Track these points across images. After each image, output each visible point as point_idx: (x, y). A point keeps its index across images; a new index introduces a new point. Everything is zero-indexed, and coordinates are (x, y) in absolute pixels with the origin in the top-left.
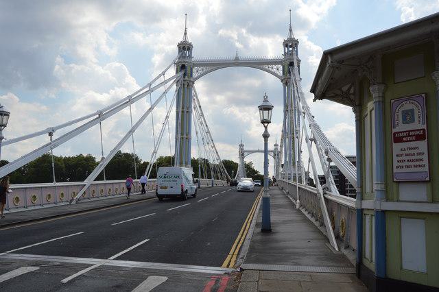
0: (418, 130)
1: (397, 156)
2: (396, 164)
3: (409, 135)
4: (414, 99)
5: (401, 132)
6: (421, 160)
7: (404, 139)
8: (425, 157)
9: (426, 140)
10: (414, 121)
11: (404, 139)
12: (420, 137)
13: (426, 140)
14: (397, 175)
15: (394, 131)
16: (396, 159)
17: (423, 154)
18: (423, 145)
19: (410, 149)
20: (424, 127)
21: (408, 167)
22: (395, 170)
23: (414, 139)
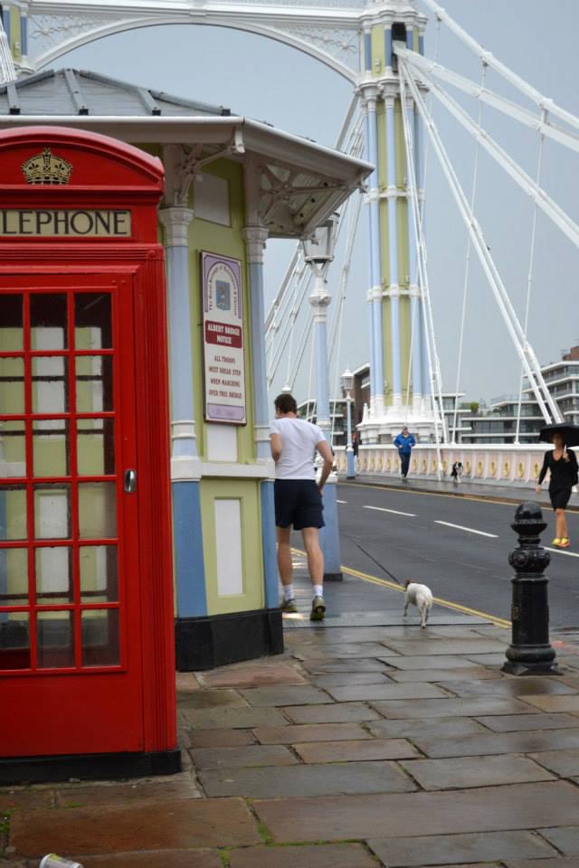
0: (234, 327)
1: (211, 369)
2: (209, 386)
3: (224, 334)
6: (237, 384)
7: (219, 339)
8: (241, 379)
10: (229, 309)
11: (219, 339)
12: (236, 342)
15: (207, 317)
16: (209, 376)
18: (237, 354)
19: (226, 360)
20: (238, 322)
21: (223, 394)
22: (210, 399)
23: (230, 343)
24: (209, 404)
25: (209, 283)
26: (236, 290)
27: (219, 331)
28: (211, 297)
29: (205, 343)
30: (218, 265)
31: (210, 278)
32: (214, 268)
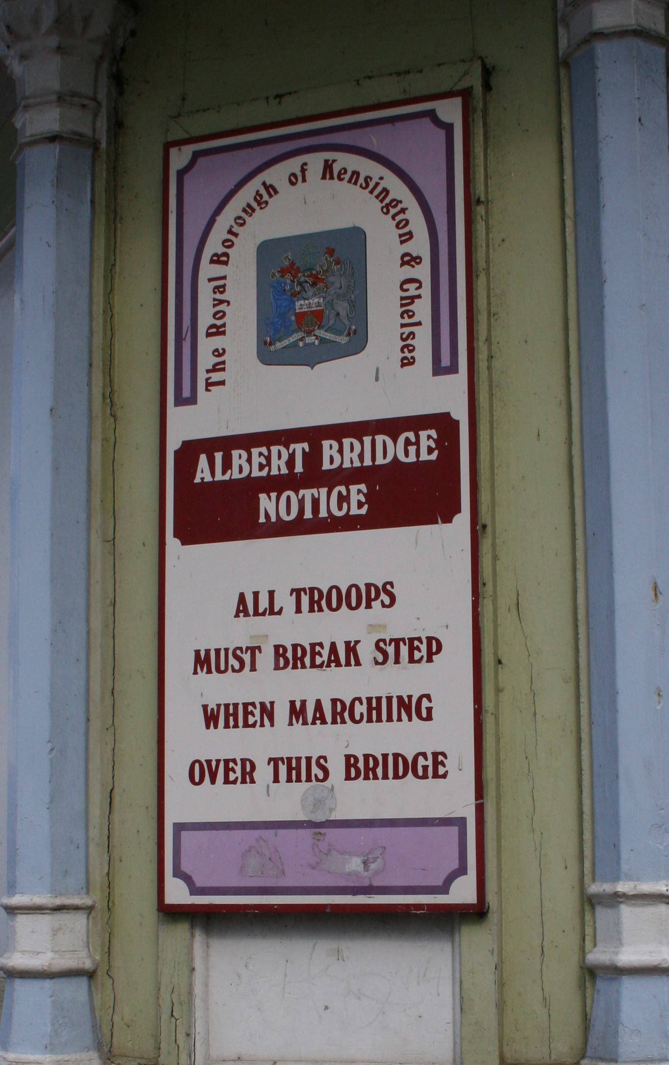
1: (202, 661)
4: (372, 139)
5: (247, 441)
7: (267, 504)
9: (463, 520)
11: (267, 504)
13: (463, 520)
14: (184, 834)
17: (434, 647)
24: (179, 828)
25: (207, 270)
26: (420, 245)
27: (279, 467)
28: (217, 331)
29: (172, 543)
30: (277, 175)
31: (213, 246)
32: (255, 185)
